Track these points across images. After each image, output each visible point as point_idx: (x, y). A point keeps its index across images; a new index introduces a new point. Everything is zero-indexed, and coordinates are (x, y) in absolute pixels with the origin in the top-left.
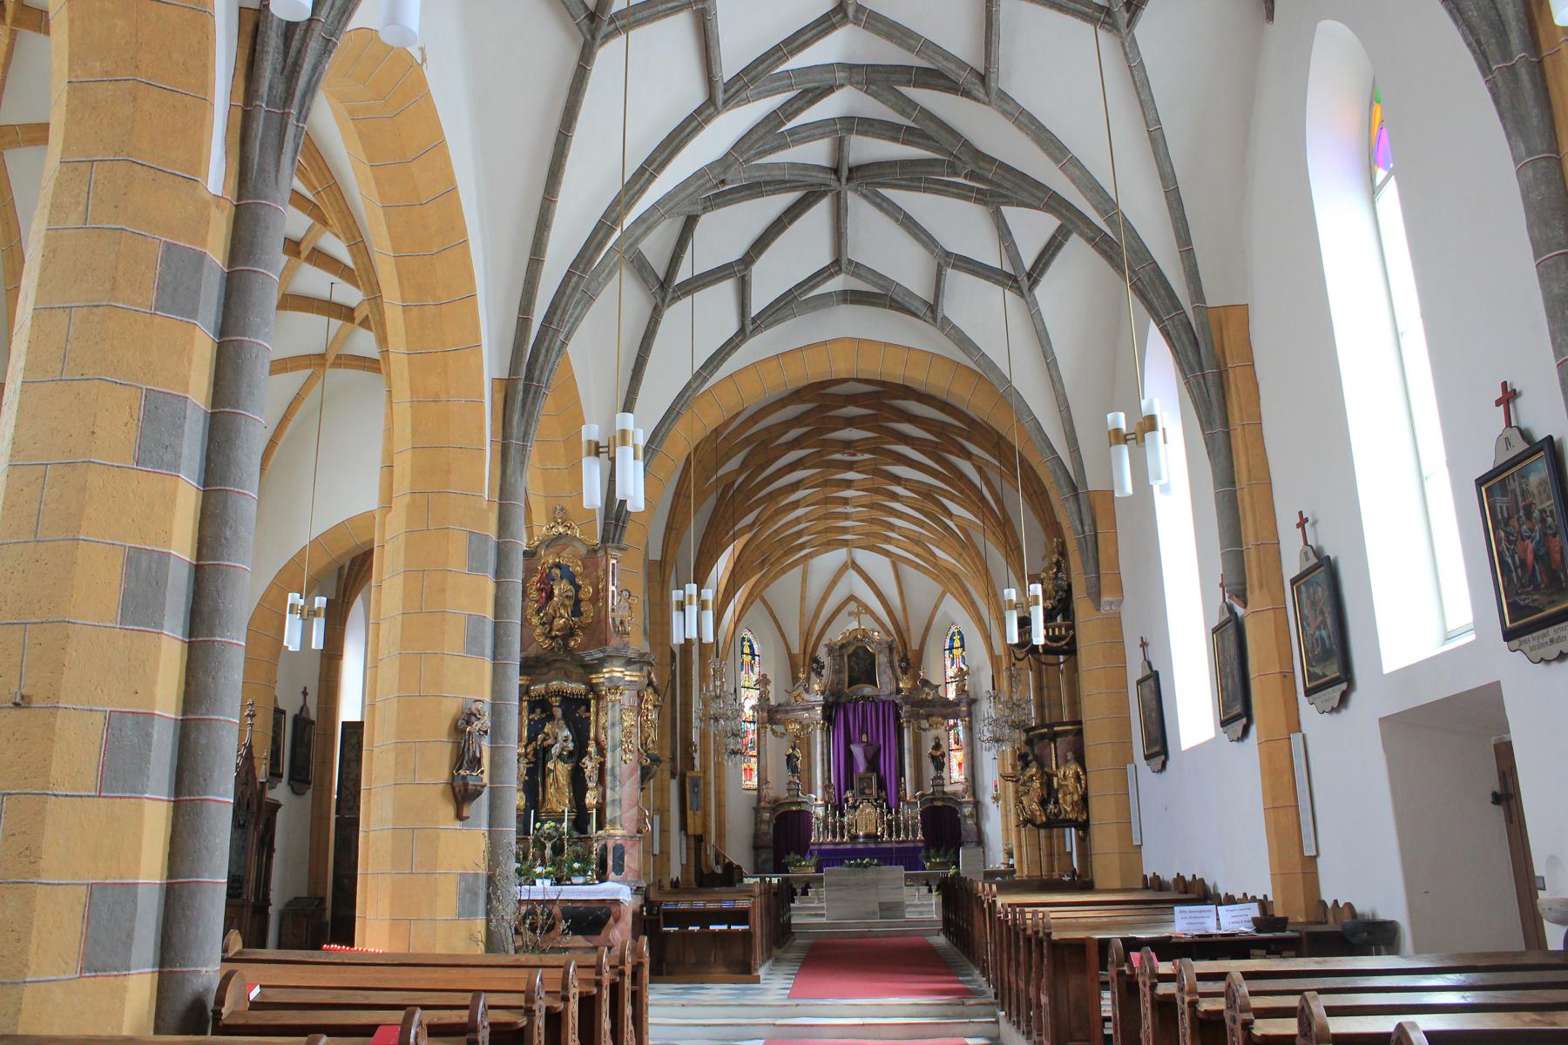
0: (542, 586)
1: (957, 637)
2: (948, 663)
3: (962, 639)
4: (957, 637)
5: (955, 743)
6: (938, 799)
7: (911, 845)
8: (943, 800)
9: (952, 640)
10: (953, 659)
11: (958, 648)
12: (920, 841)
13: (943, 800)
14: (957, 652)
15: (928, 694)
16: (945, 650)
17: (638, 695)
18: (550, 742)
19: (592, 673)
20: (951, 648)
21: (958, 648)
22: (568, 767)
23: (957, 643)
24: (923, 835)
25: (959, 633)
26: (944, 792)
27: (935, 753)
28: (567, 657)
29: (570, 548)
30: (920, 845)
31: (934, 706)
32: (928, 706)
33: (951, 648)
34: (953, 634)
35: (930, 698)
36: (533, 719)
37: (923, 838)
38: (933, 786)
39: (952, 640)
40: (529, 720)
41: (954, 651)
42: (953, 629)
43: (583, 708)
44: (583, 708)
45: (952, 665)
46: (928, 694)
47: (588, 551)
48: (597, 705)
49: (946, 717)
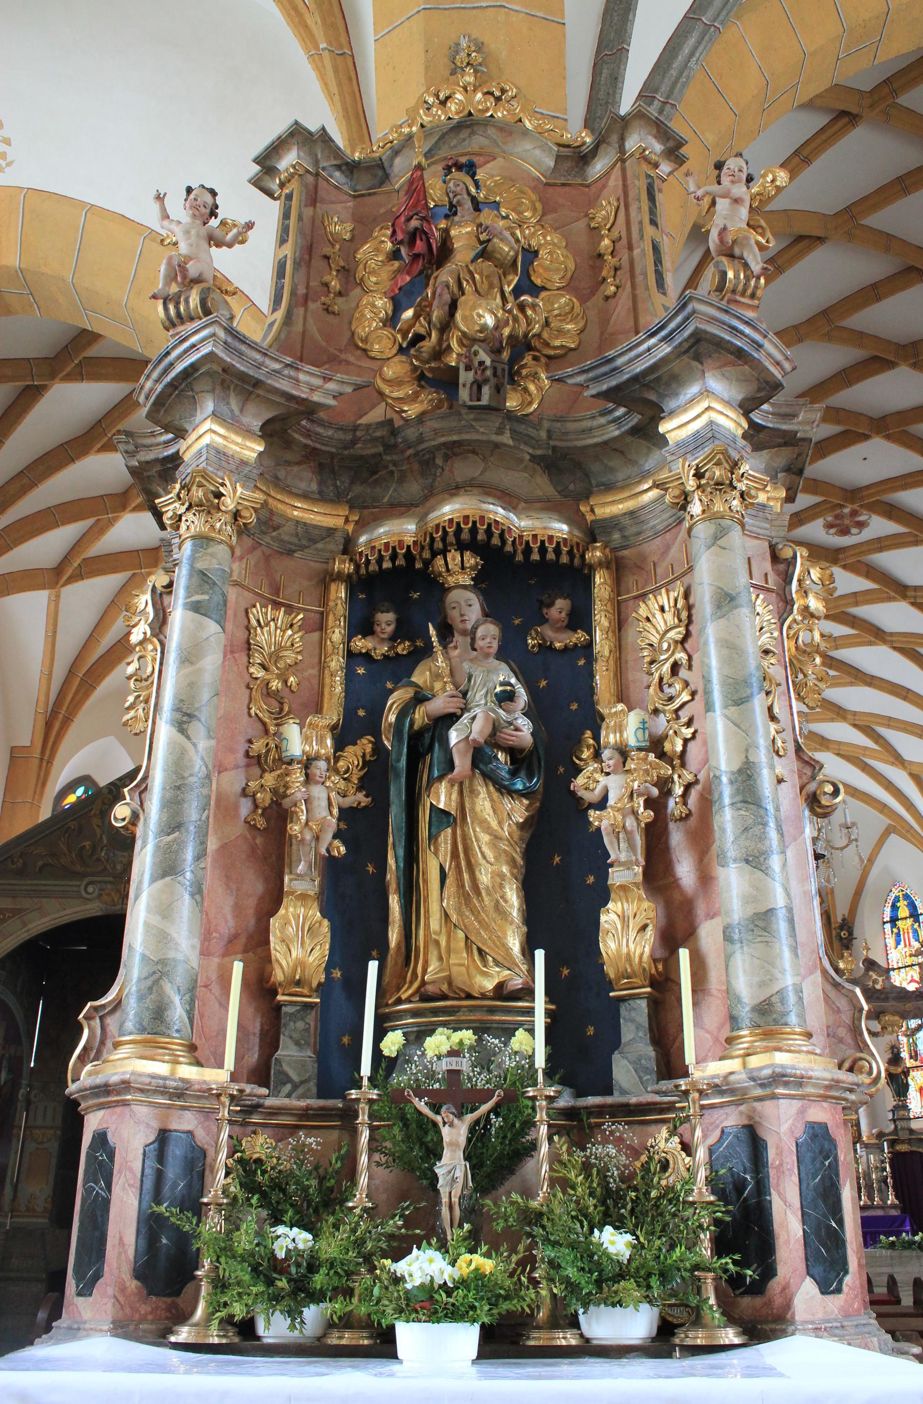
0: (414, 223)
1: (902, 904)
2: (891, 941)
3: (912, 906)
4: (902, 904)
5: (911, 1057)
6: (903, 1142)
7: (880, 1213)
8: (909, 1142)
9: (895, 908)
10: (898, 935)
11: (906, 918)
12: (893, 1206)
13: (909, 1142)
14: (905, 925)
15: (875, 982)
16: (884, 923)
17: (775, 558)
18: (439, 705)
19: (586, 495)
20: (894, 920)
21: (906, 918)
22: (518, 810)
23: (904, 912)
24: (897, 1197)
25: (906, 897)
26: (912, 1131)
27: (893, 1070)
28: (500, 432)
29: (500, 161)
30: (894, 1212)
31: (886, 999)
32: (878, 998)
33: (894, 920)
34: (897, 899)
35: (878, 987)
36: (367, 657)
37: (897, 1202)
38: (894, 1120)
39: (895, 908)
40: (351, 655)
41: (899, 923)
42: (895, 892)
43: (560, 608)
44: (560, 608)
45: (898, 943)
46: (875, 982)
47: (559, 158)
48: (618, 585)
49: (905, 1016)
